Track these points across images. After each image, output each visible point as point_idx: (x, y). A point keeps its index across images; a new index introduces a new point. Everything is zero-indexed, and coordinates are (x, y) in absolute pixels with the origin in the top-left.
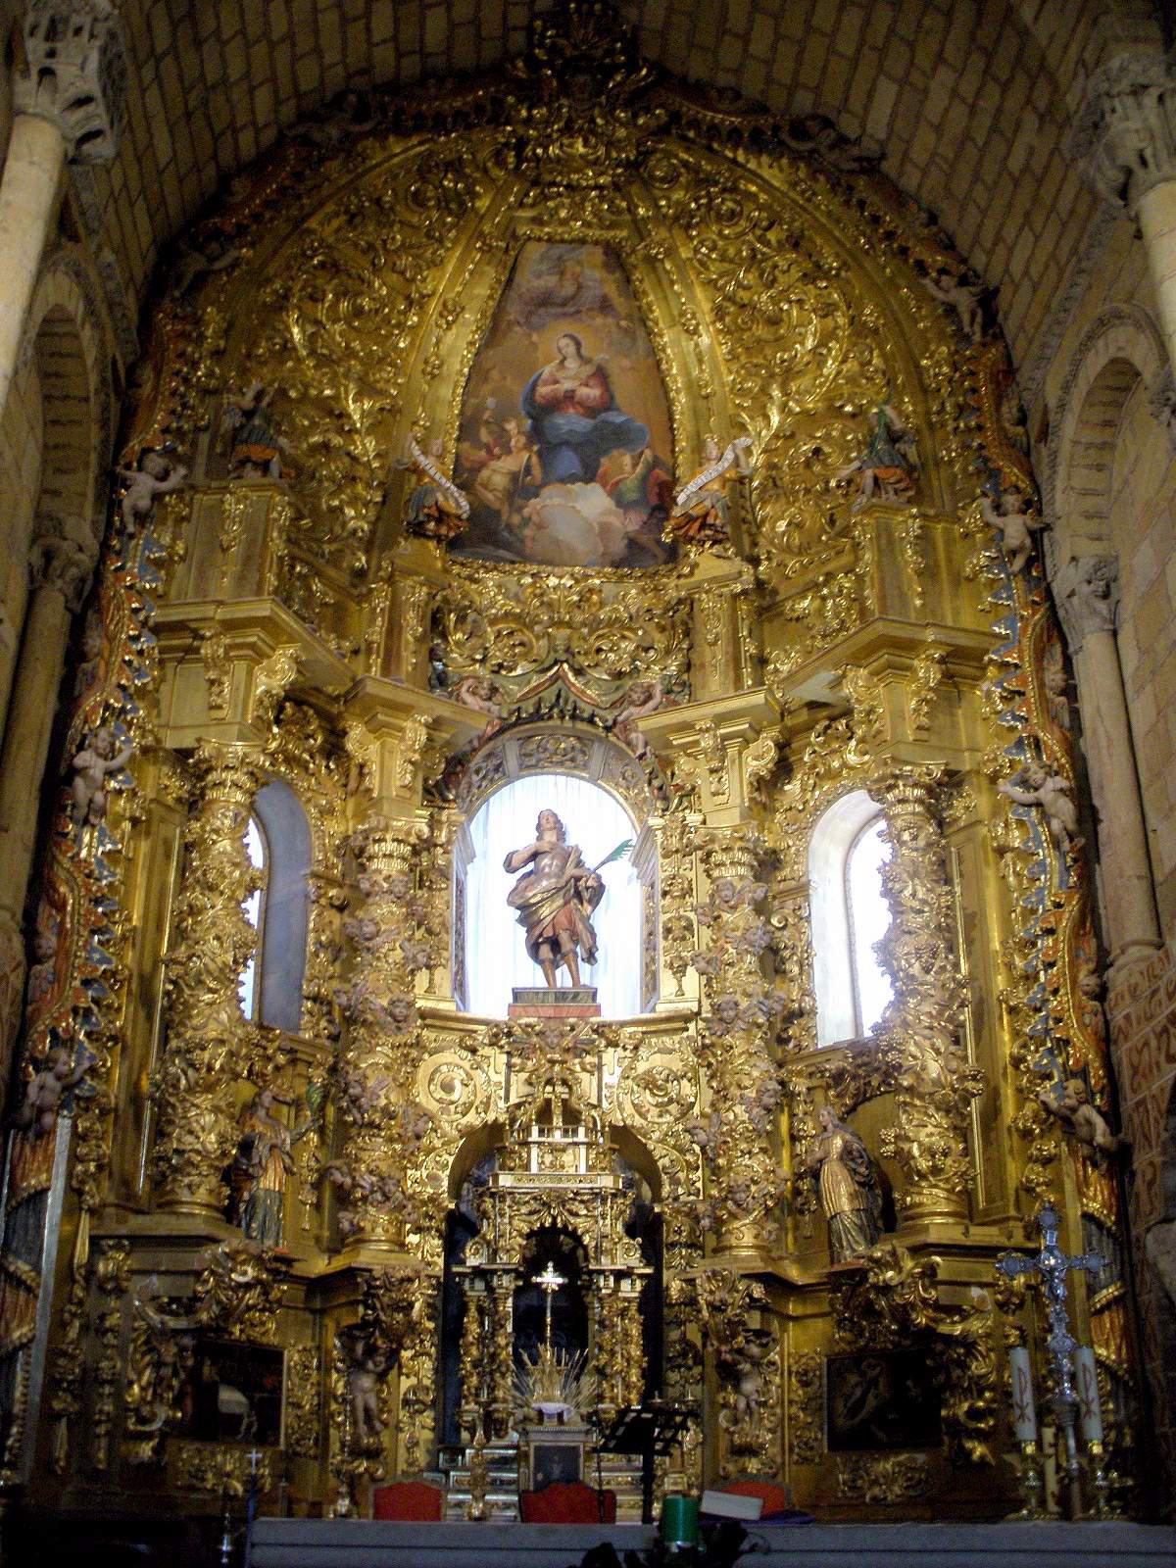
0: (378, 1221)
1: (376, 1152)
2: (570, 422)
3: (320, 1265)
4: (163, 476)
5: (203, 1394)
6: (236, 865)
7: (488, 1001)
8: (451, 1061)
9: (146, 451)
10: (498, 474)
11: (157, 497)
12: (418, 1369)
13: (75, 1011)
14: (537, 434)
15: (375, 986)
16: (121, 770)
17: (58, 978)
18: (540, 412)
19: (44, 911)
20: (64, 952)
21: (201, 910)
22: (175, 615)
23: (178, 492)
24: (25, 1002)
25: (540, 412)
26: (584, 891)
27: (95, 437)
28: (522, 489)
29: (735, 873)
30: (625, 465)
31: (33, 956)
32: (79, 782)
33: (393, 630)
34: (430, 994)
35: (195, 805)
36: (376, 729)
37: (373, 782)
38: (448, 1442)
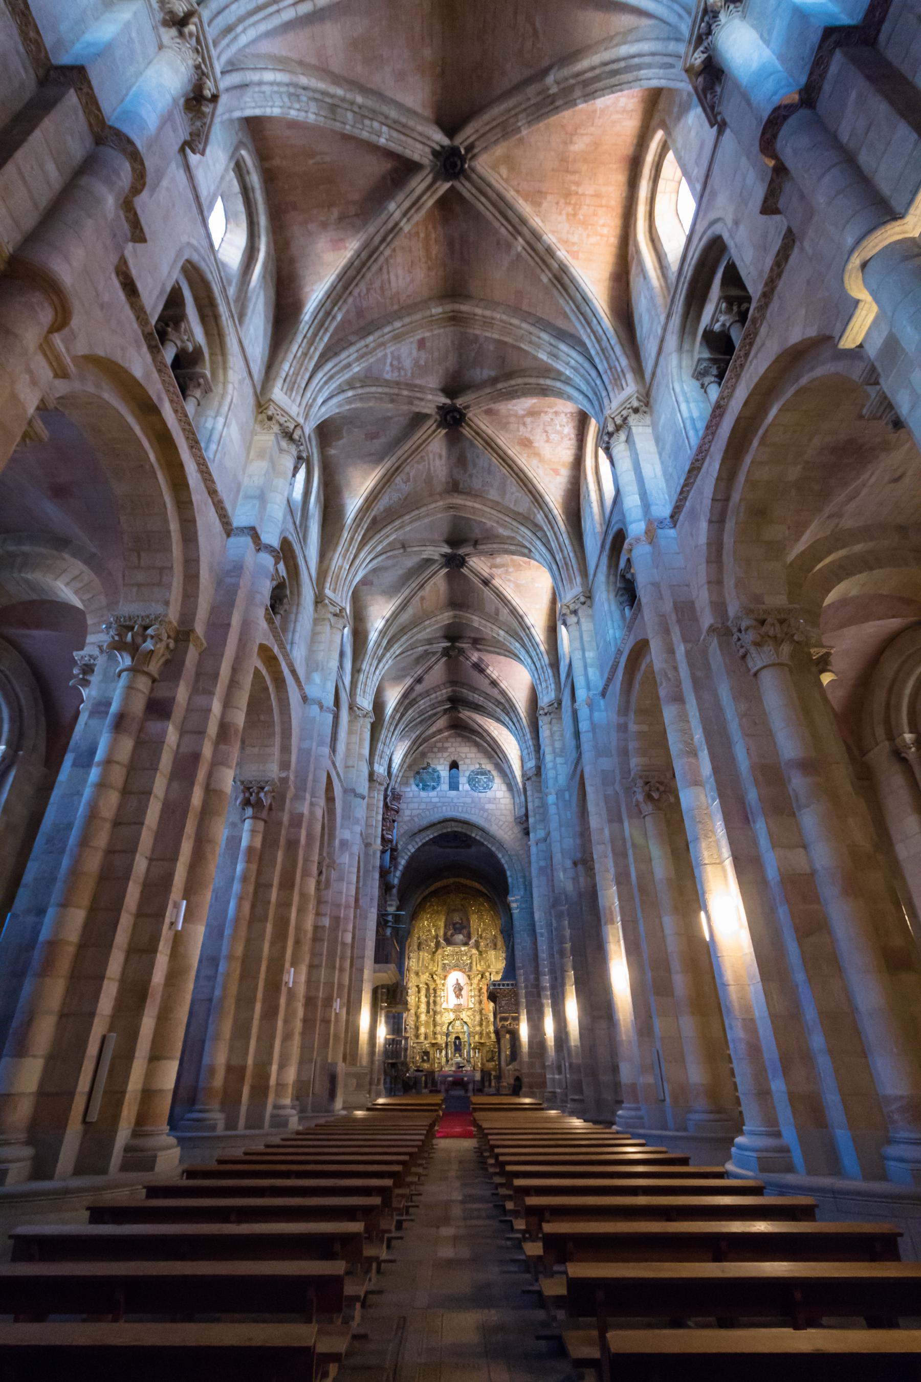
0: (439, 1036)
1: (438, 1028)
2: (458, 926)
3: (434, 1041)
5: (423, 1058)
7: (451, 1006)
8: (446, 1014)
10: (449, 933)
12: (444, 1052)
14: (455, 929)
15: (438, 1009)
18: (454, 924)
25: (454, 924)
26: (461, 989)
28: (452, 935)
29: (477, 993)
30: (465, 931)
34: (444, 1006)
38: (447, 1061)
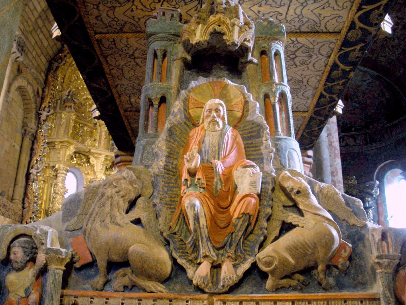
4: (49, 112)
6: (62, 189)
9: (45, 107)
11: (47, 116)
13: (31, 218)
16: (40, 172)
17: (28, 211)
19: (26, 199)
20: (29, 207)
21: (56, 197)
22: (50, 141)
23: (53, 114)
24: (22, 216)
27: (34, 106)
31: (24, 208)
32: (31, 175)
33: (100, 136)
35: (56, 176)
36: (95, 158)
37: (95, 169)
